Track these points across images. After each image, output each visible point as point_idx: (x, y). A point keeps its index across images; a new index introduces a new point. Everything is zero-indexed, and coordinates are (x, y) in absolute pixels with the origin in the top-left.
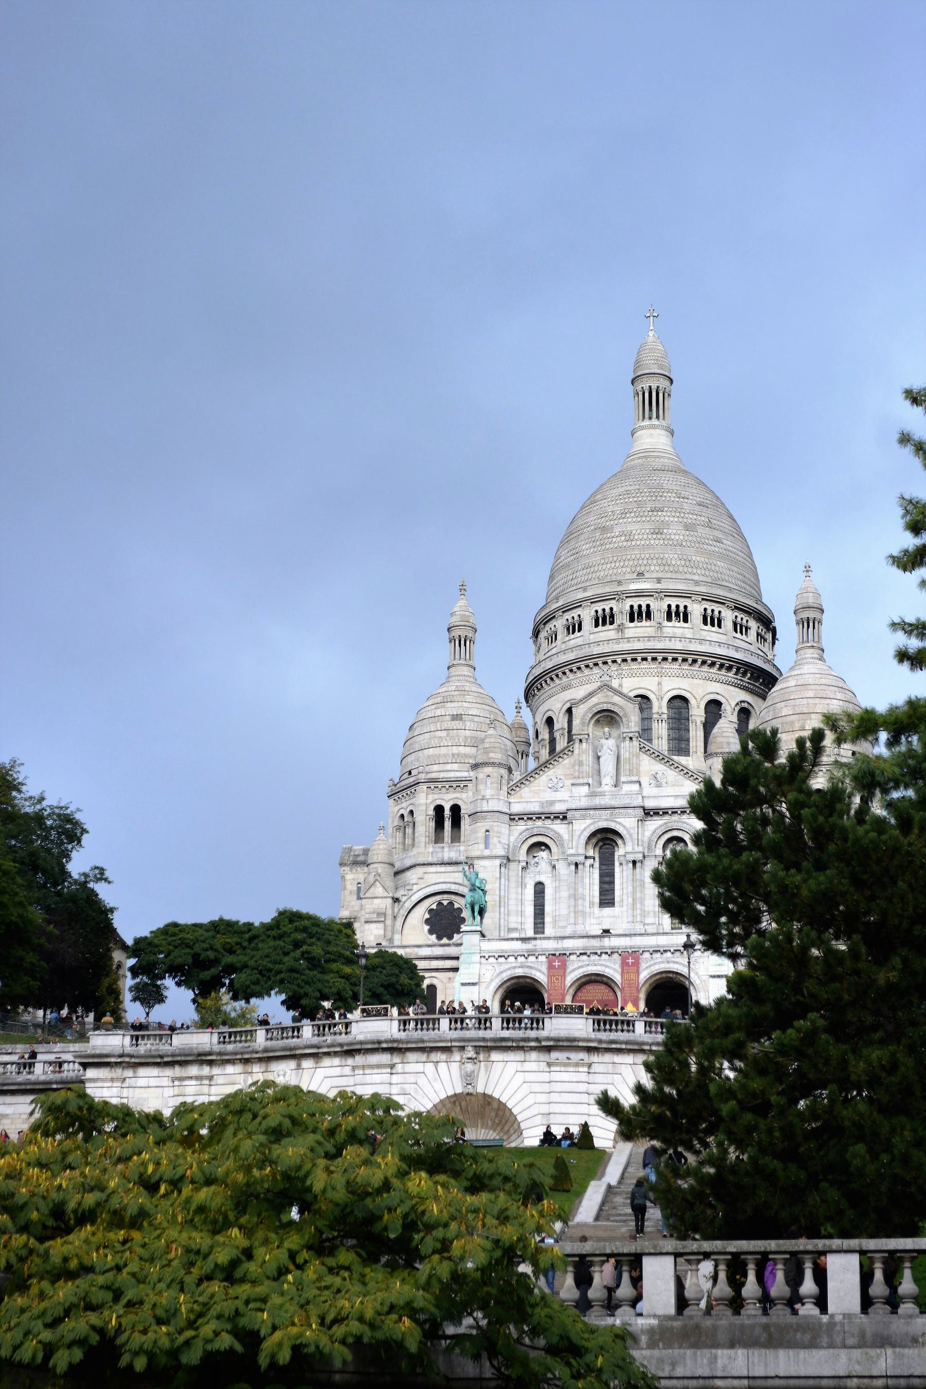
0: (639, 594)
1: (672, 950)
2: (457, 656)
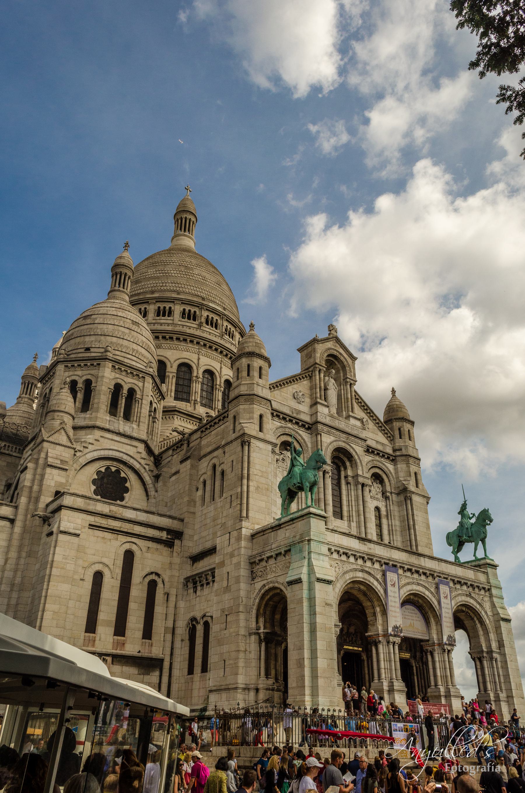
0: (213, 311)
1: (469, 584)
2: (122, 286)
